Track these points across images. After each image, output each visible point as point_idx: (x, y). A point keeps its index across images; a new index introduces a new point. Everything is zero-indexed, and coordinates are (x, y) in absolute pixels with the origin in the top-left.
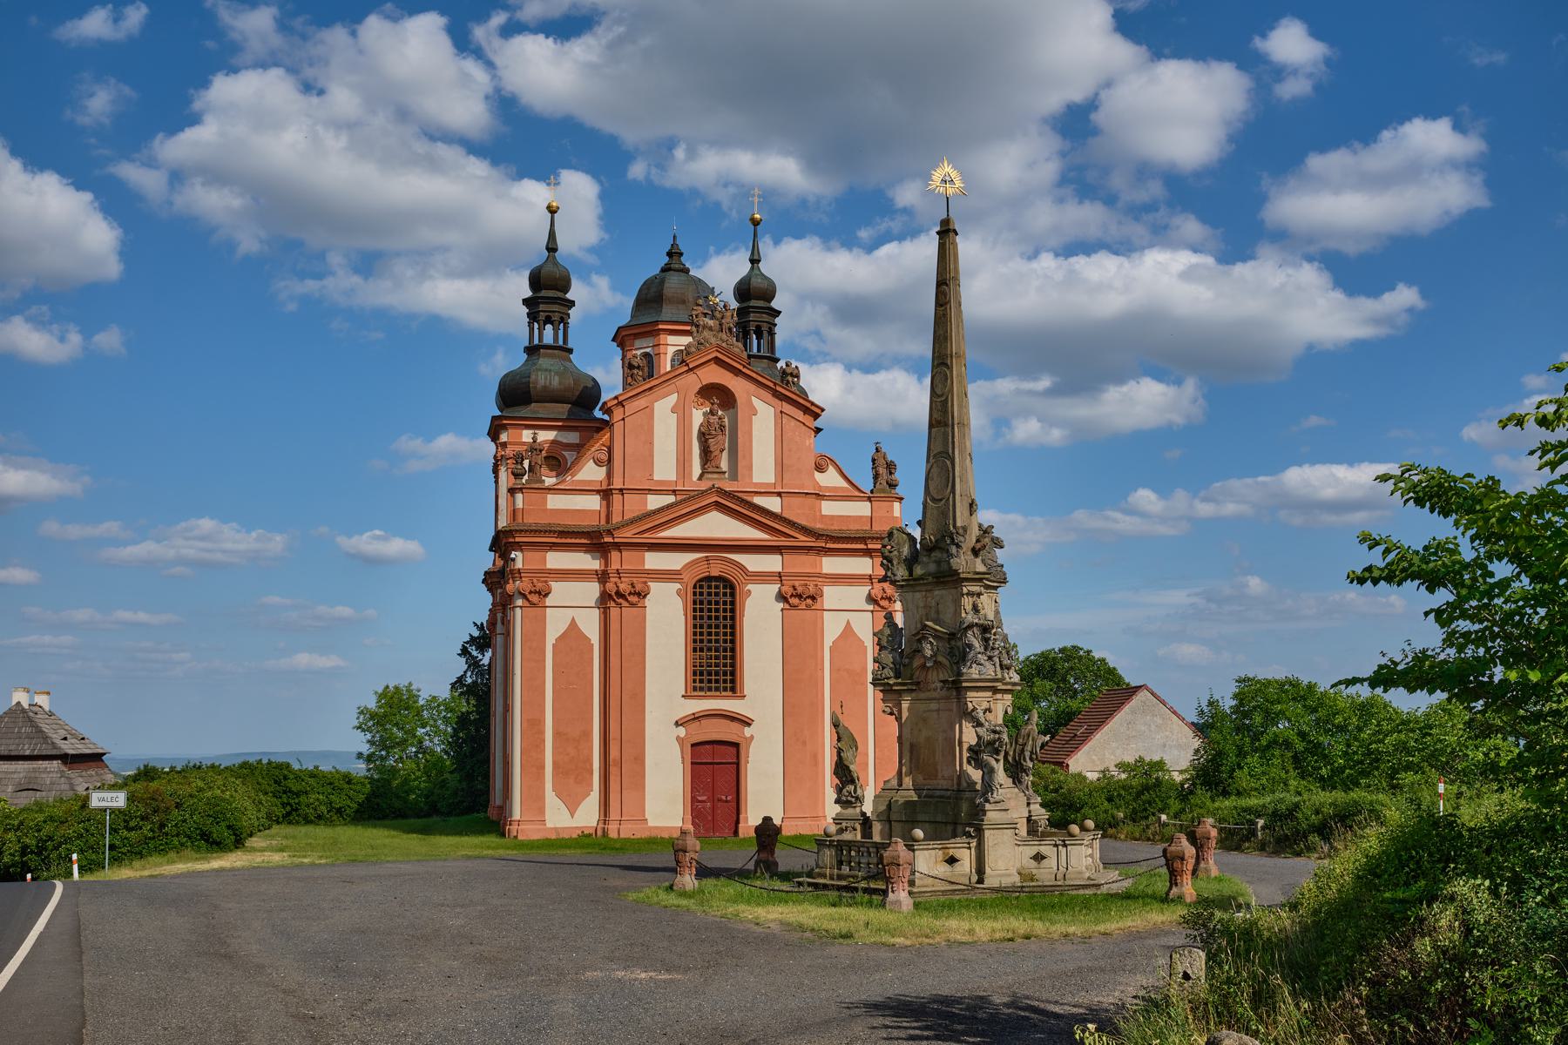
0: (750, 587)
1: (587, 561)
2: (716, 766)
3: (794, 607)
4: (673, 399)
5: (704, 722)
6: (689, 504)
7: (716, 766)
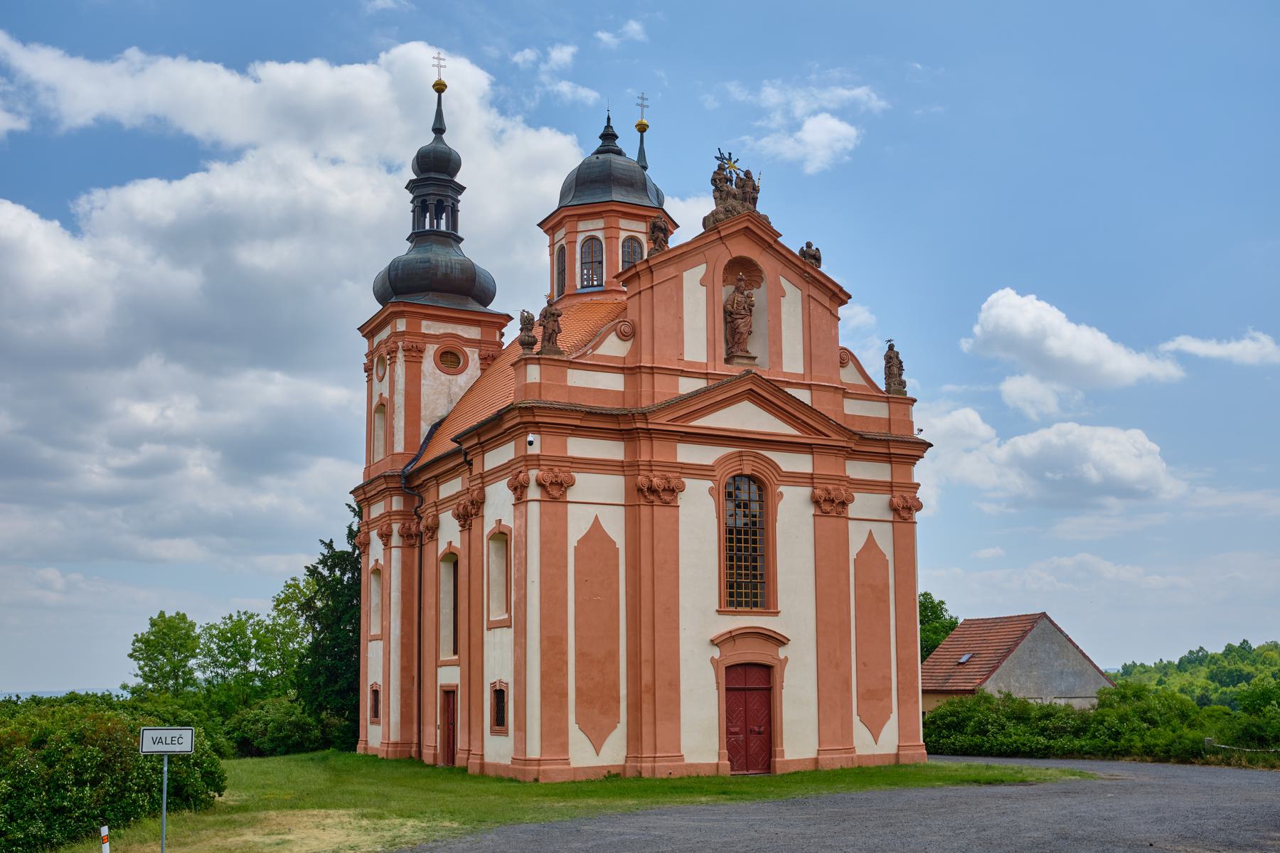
0: (782, 489)
1: (613, 450)
2: (750, 692)
3: (826, 513)
4: (701, 270)
5: (739, 641)
6: (720, 393)
7: (750, 692)
